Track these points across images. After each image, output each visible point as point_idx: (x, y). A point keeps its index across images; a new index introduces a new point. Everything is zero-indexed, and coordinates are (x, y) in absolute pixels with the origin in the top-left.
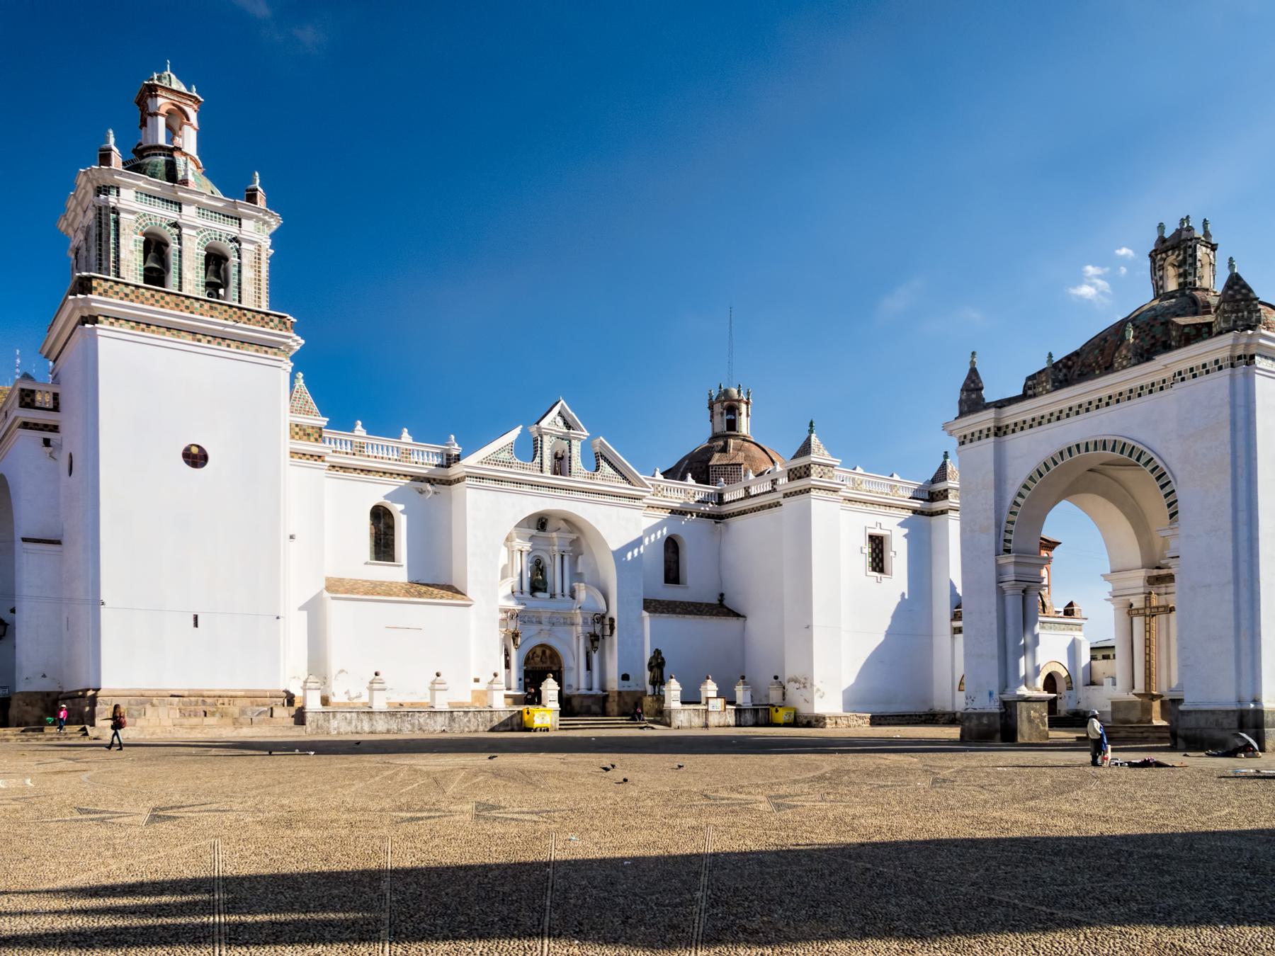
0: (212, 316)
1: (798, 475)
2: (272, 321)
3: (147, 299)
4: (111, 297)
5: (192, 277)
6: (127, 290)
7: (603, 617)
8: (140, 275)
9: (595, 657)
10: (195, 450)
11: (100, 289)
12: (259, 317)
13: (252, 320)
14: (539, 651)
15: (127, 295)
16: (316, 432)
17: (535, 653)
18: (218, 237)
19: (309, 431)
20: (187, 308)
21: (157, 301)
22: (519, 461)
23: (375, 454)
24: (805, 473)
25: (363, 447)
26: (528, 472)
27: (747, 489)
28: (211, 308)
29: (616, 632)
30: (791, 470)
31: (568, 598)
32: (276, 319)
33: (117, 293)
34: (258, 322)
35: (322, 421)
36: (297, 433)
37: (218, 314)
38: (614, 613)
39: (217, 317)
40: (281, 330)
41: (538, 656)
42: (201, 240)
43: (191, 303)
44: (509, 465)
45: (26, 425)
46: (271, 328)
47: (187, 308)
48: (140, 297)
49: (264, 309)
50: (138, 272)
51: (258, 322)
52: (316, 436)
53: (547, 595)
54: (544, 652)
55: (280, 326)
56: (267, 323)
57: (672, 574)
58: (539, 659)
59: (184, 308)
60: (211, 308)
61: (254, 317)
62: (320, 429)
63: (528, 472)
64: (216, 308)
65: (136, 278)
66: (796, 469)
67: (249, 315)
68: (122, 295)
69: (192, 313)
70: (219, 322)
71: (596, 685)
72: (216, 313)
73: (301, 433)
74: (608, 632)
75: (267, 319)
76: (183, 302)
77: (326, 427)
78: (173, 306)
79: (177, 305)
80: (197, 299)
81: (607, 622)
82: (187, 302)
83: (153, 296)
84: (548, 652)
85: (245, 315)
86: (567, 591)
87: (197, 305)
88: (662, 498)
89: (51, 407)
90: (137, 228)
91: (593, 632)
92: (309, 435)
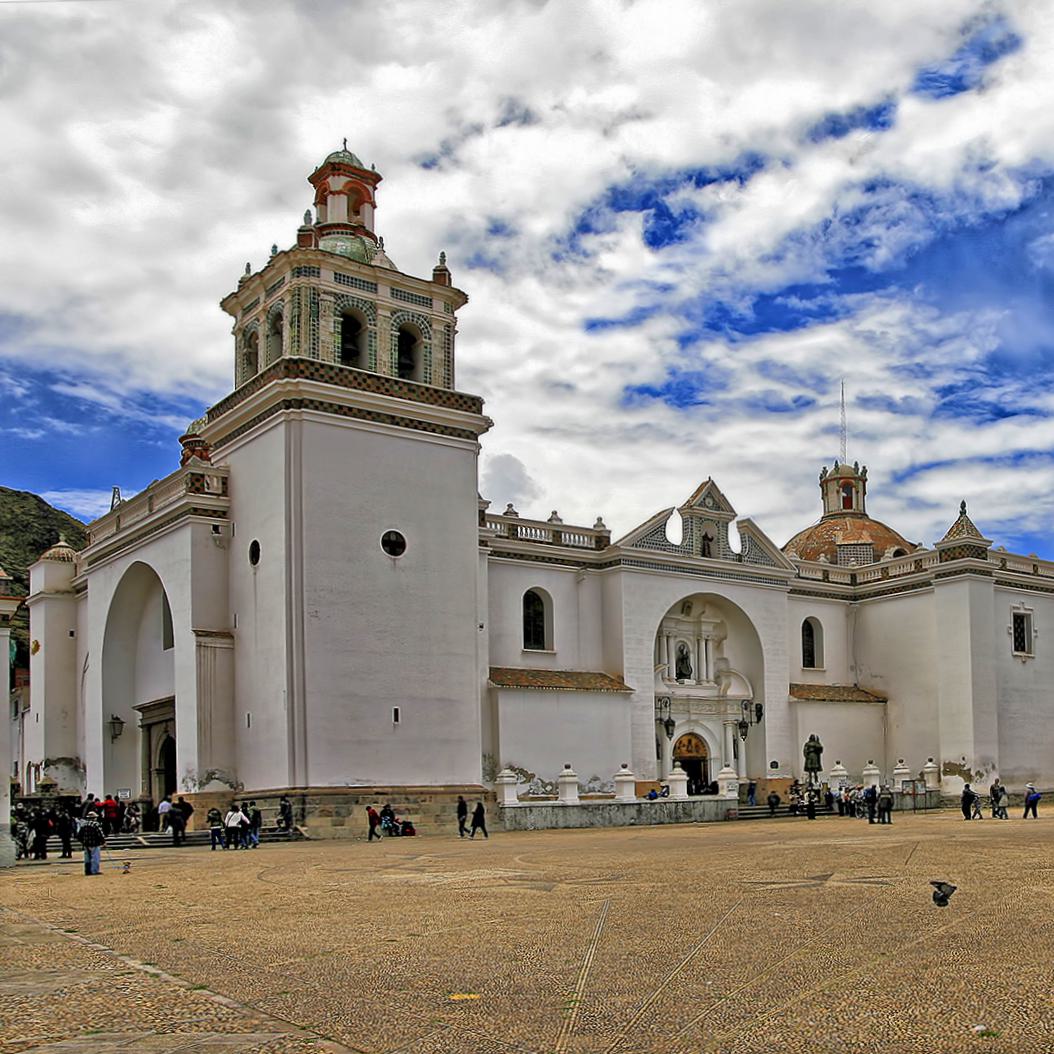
1: (952, 556)
3: (350, 382)
5: (382, 355)
7: (750, 702)
8: (339, 357)
9: (742, 744)
10: (393, 538)
11: (307, 373)
14: (685, 742)
15: (331, 378)
17: (681, 742)
18: (411, 318)
20: (387, 390)
21: (359, 384)
24: (960, 553)
27: (885, 570)
30: (943, 551)
31: (712, 684)
41: (684, 746)
42: (395, 321)
48: (345, 380)
54: (690, 741)
57: (810, 659)
58: (685, 749)
59: (384, 391)
66: (949, 549)
68: (327, 378)
71: (743, 774)
74: (755, 719)
84: (694, 741)
85: (440, 397)
86: (711, 677)
87: (396, 388)
89: (220, 492)
90: (336, 309)
91: (741, 719)
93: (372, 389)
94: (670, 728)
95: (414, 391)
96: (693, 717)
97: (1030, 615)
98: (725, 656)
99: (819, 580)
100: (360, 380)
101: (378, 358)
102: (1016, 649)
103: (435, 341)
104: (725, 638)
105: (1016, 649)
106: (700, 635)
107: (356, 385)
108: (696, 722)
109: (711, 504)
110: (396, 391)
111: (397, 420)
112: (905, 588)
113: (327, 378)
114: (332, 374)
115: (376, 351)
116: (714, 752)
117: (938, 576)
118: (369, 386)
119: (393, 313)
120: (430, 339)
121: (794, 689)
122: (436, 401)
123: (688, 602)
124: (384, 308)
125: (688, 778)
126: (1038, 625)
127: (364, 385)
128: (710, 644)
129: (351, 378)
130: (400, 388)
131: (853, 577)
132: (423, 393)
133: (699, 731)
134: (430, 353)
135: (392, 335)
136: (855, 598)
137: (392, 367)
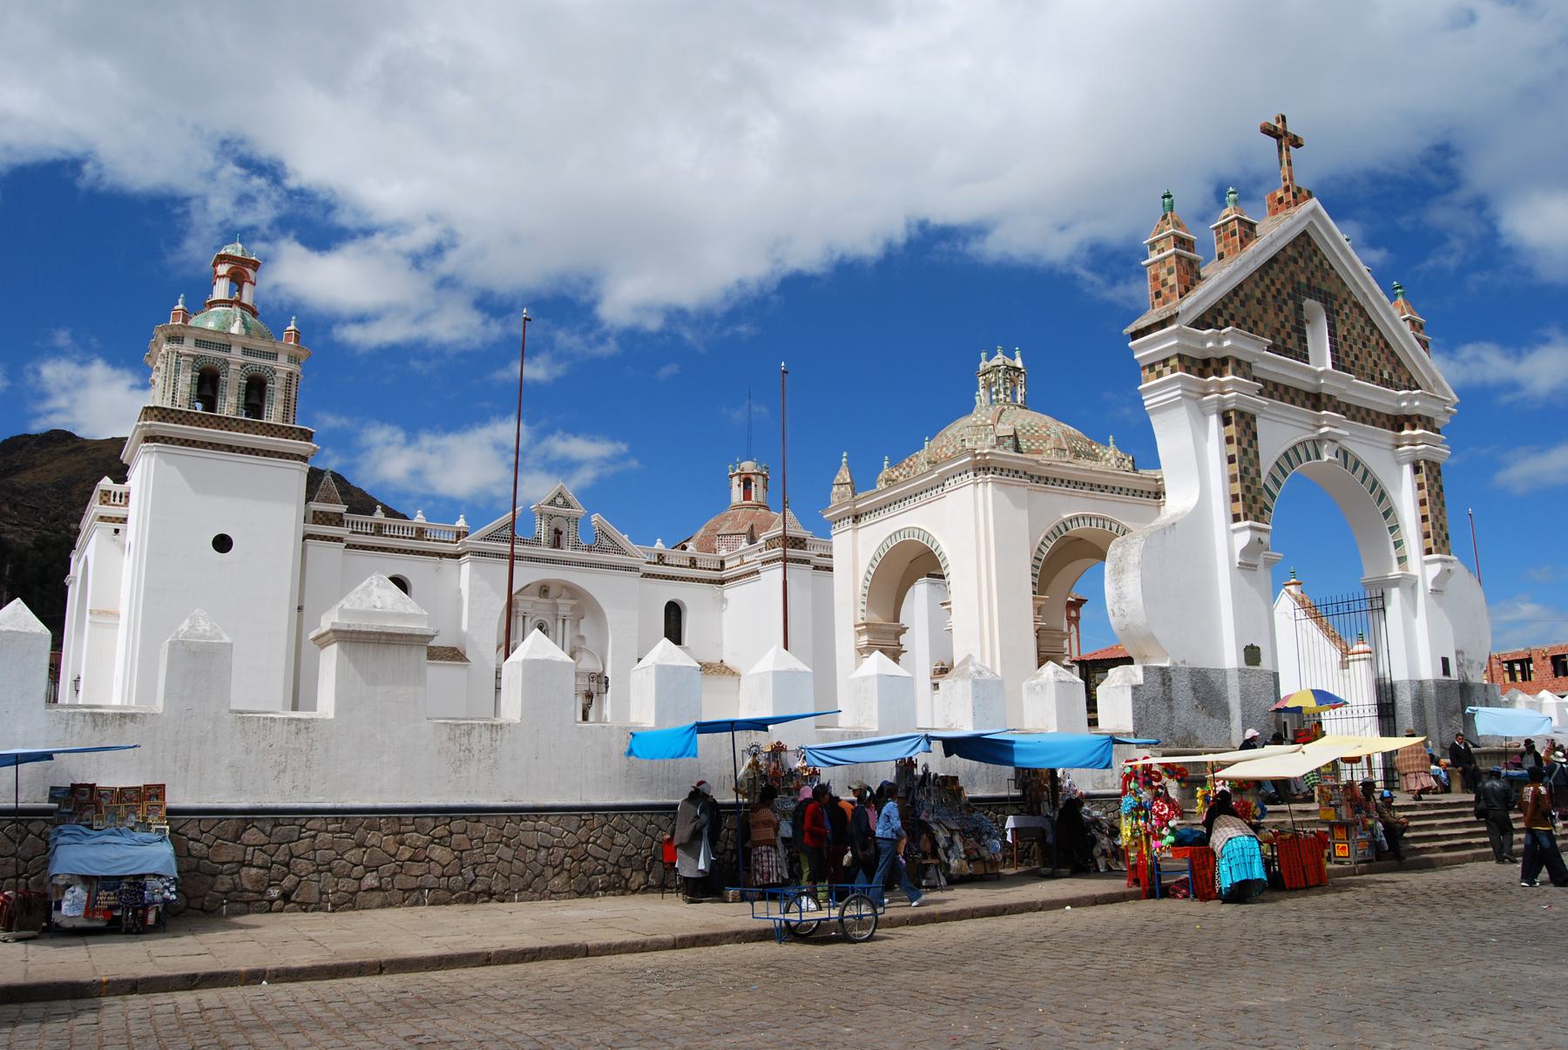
0: (245, 432)
2: (294, 432)
3: (196, 421)
4: (168, 422)
6: (181, 416)
15: (180, 419)
21: (203, 423)
23: (392, 534)
29: (609, 689)
33: (172, 418)
34: (283, 434)
35: (342, 508)
36: (321, 519)
38: (608, 674)
39: (250, 433)
40: (301, 440)
45: (102, 518)
46: (294, 439)
47: (226, 426)
51: (283, 434)
52: (337, 520)
55: (302, 436)
56: (290, 435)
62: (341, 514)
68: (176, 419)
69: (230, 430)
73: (324, 519)
87: (234, 424)
92: (331, 520)
95: (249, 426)
98: (582, 633)
99: (686, 567)
100: (203, 419)
103: (276, 386)
104: (583, 618)
106: (557, 615)
111: (233, 448)
113: (176, 419)
114: (181, 416)
118: (211, 424)
119: (243, 366)
120: (274, 384)
122: (268, 432)
123: (545, 586)
124: (235, 363)
127: (207, 423)
128: (567, 623)
129: (196, 418)
130: (238, 424)
131: (722, 563)
132: (257, 427)
136: (722, 582)
137: (238, 407)
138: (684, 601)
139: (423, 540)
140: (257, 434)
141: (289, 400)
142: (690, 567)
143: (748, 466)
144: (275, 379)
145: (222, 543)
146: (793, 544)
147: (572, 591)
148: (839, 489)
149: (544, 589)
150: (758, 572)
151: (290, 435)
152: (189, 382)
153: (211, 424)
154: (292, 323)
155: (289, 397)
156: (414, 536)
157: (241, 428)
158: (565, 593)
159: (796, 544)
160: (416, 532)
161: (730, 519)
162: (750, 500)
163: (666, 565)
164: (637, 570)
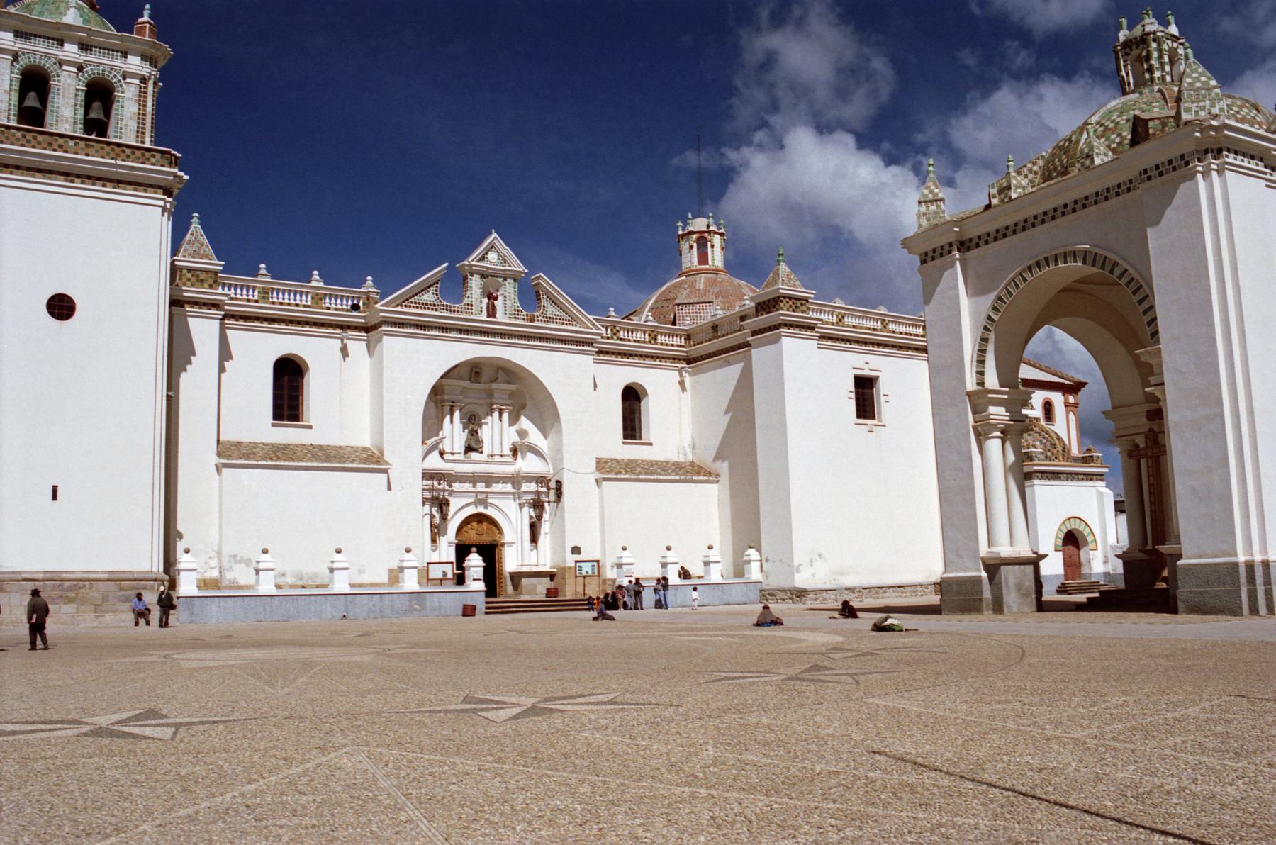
0: (87, 155)
2: (153, 156)
3: (18, 139)
8: (14, 115)
12: (138, 153)
13: (132, 156)
16: (211, 278)
19: (202, 276)
20: (60, 146)
22: (445, 303)
23: (281, 300)
25: (268, 293)
26: (455, 315)
28: (87, 146)
32: (158, 156)
35: (216, 264)
36: (189, 280)
37: (93, 153)
39: (93, 156)
40: (162, 166)
43: (65, 141)
44: (433, 307)
46: (153, 164)
47: (60, 146)
49: (148, 145)
50: (12, 112)
52: (211, 281)
53: (483, 457)
56: (148, 159)
57: (632, 428)
59: (57, 147)
60: (87, 146)
61: (133, 153)
62: (216, 272)
63: (455, 315)
64: (92, 146)
65: (9, 119)
67: (128, 151)
69: (65, 152)
70: (98, 160)
72: (92, 151)
75: (148, 155)
76: (57, 141)
77: (222, 272)
78: (46, 145)
79: (50, 144)
80: (72, 138)
81: (553, 485)
82: (61, 141)
83: (24, 136)
85: (124, 151)
87: (71, 143)
88: (619, 342)
93: (43, 145)
94: (444, 508)
96: (481, 496)
97: (877, 377)
99: (644, 342)
101: (60, 113)
102: (859, 416)
105: (859, 416)
107: (24, 143)
108: (485, 503)
109: (496, 260)
110: (71, 147)
112: (732, 349)
115: (58, 107)
116: (508, 536)
117: (754, 333)
118: (39, 143)
120: (123, 92)
121: (601, 464)
123: (476, 367)
125: (484, 564)
126: (884, 387)
133: (490, 512)
134: (122, 107)
135: (77, 90)
138: (647, 388)
139: (322, 308)
140: (103, 157)
141: (144, 115)
142: (650, 342)
143: (699, 224)
144: (124, 86)
145: (61, 307)
146: (793, 306)
147: (508, 372)
148: (928, 207)
149: (475, 370)
150: (747, 345)
151: (148, 159)
152: (7, 88)
153: (39, 143)
154: (146, 13)
155: (145, 110)
156: (309, 303)
157: (82, 149)
158: (501, 375)
159: (796, 307)
160: (313, 298)
161: (686, 286)
162: (707, 264)
163: (621, 339)
164: (590, 343)
